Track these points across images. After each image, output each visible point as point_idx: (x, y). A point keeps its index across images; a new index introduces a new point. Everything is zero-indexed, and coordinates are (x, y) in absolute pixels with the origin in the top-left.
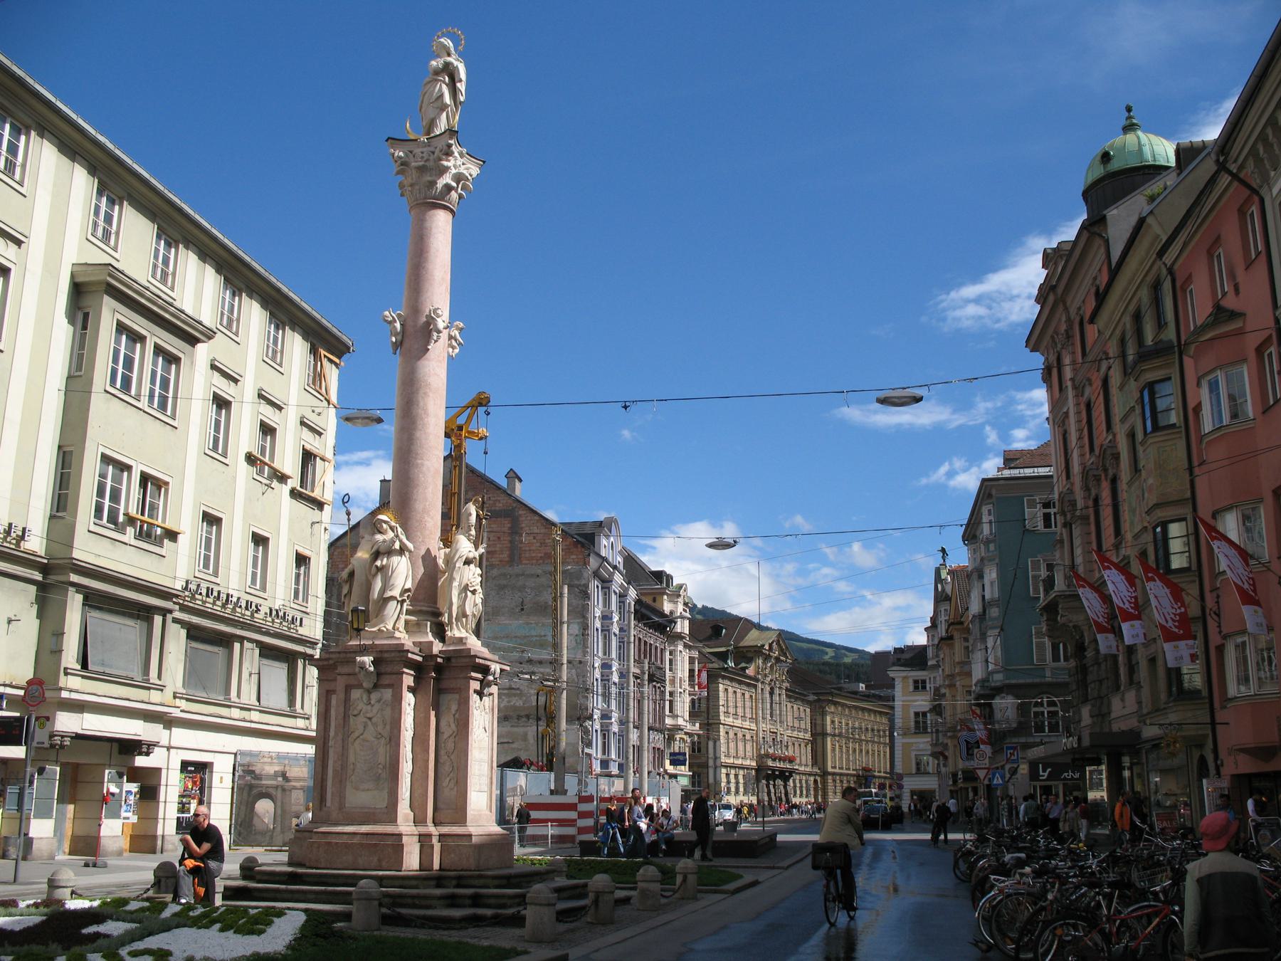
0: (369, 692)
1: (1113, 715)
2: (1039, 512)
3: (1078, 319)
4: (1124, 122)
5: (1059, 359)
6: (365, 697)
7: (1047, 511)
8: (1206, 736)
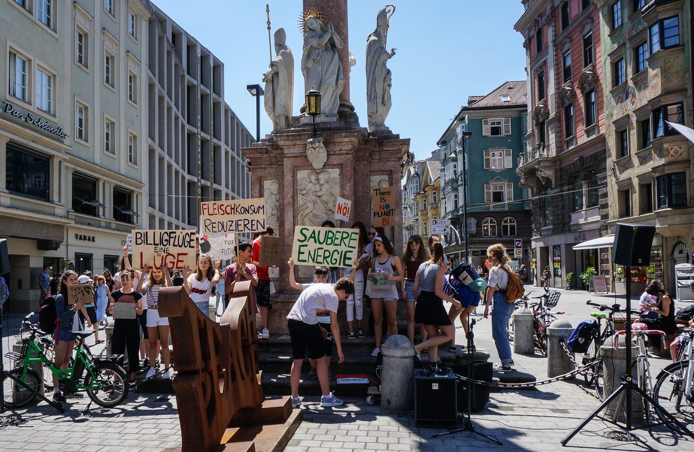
1: (572, 223)
6: (313, 177)
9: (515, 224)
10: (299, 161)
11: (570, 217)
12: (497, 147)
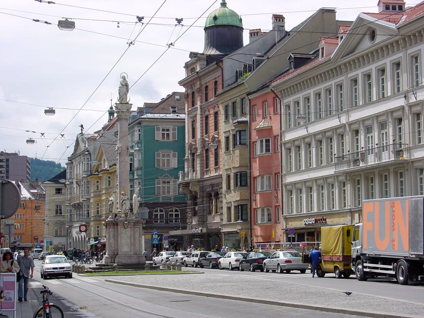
1: (208, 222)
2: (161, 132)
3: (205, 86)
5: (193, 93)
7: (163, 132)
8: (248, 232)
9: (179, 213)
11: (207, 218)
12: (166, 150)
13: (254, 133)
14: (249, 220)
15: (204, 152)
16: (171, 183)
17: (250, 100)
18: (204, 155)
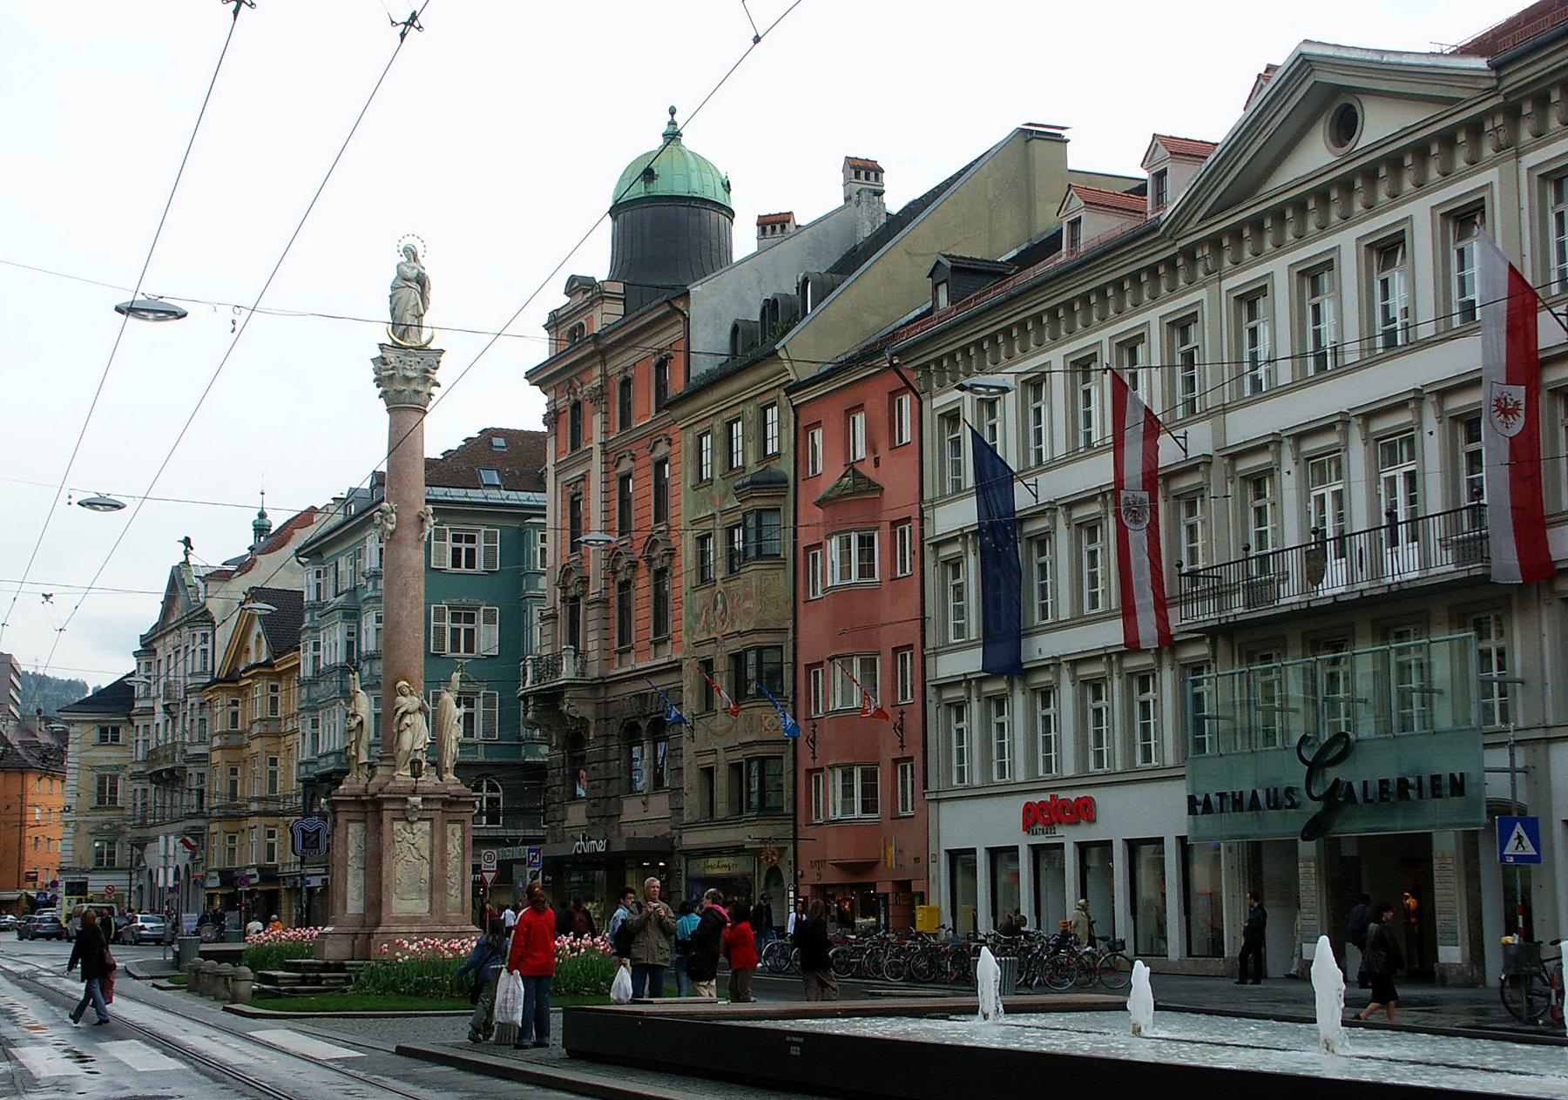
0: (412, 823)
1: (623, 818)
2: (449, 544)
3: (619, 379)
4: (665, 128)
5: (576, 406)
7: (457, 545)
10: (398, 815)
13: (811, 515)
14: (788, 809)
15: (614, 592)
16: (479, 704)
17: (794, 408)
18: (615, 601)
